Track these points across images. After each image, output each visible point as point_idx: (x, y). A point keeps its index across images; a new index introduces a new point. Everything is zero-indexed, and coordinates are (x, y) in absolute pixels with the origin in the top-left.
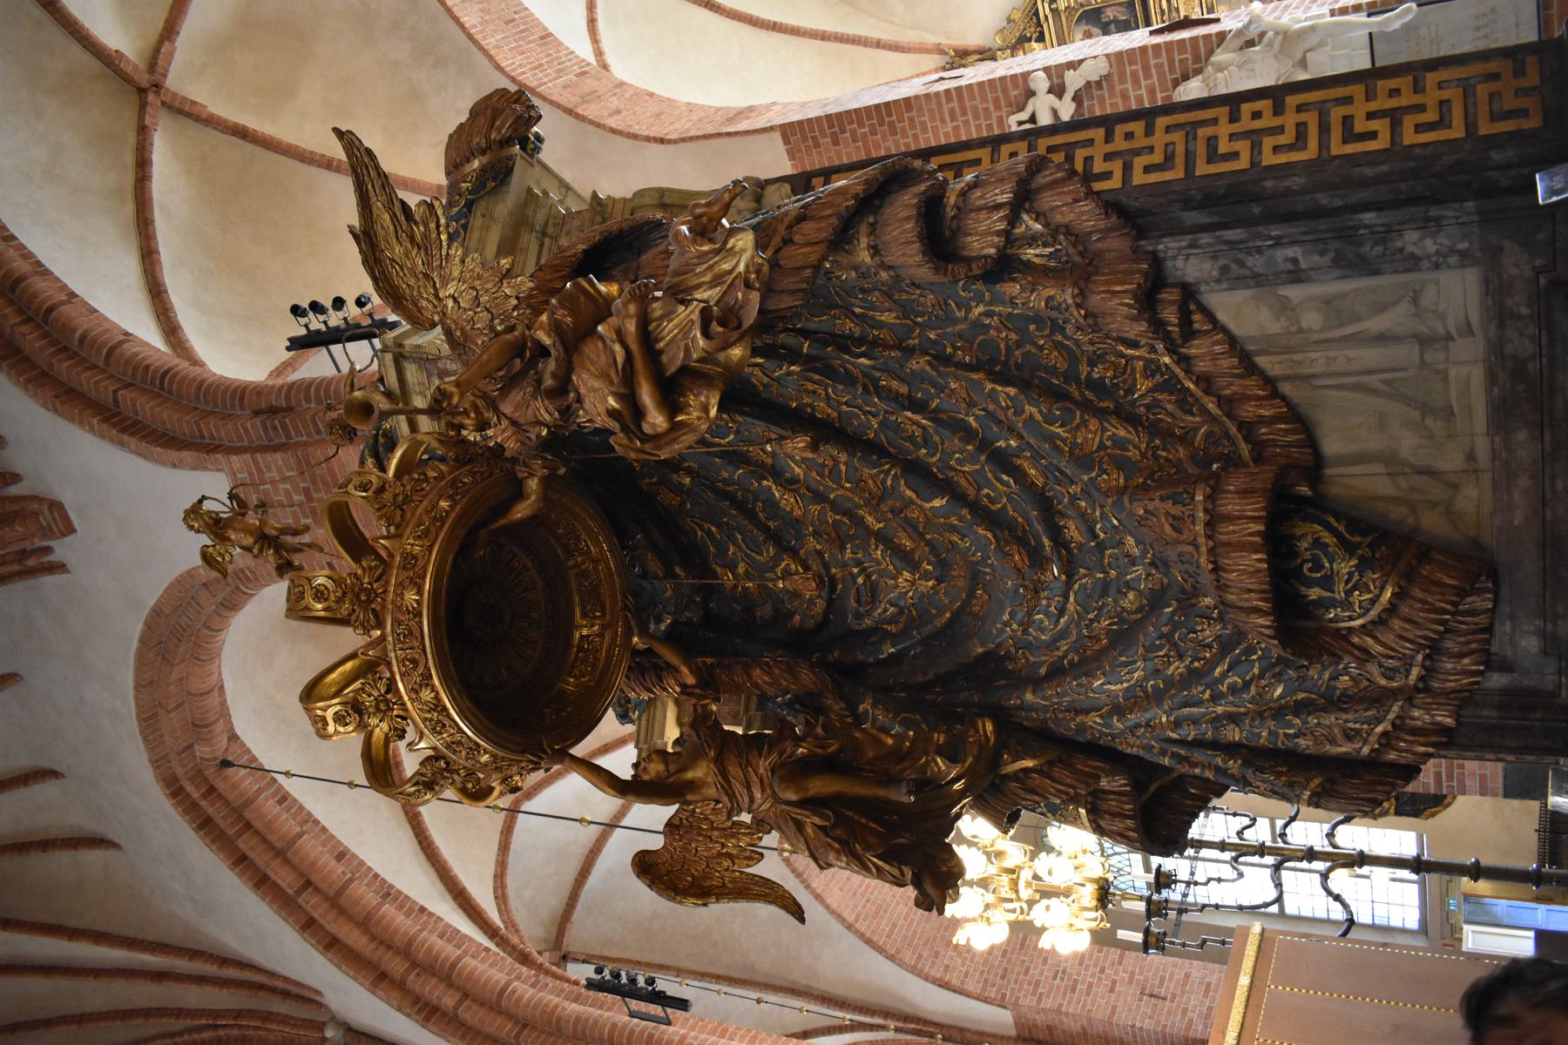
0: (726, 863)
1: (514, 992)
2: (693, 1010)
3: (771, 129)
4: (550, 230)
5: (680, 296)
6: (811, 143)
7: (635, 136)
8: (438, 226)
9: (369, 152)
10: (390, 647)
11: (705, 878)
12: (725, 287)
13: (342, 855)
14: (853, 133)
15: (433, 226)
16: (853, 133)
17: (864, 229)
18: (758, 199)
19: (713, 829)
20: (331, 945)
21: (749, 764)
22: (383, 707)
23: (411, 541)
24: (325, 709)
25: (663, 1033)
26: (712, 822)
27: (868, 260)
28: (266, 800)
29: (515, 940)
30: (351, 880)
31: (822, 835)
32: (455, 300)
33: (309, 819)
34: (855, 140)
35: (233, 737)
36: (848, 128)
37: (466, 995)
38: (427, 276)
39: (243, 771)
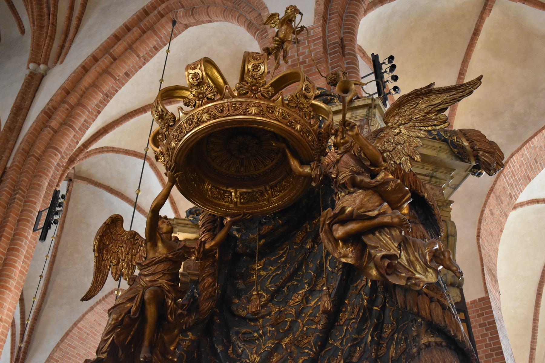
0: (114, 262)
1: (56, 155)
2: (39, 243)
3: (487, 292)
4: (434, 180)
5: (402, 244)
6: (480, 312)
7: (480, 222)
8: (435, 125)
9: (471, 92)
10: (229, 100)
11: (107, 251)
12: (407, 267)
13: (128, 75)
14: (486, 335)
15: (435, 123)
16: (486, 335)
17: (439, 340)
18: (452, 285)
19: (132, 256)
20: (85, 69)
21: (164, 274)
22: (201, 96)
23: (281, 111)
24: (200, 69)
25: (29, 228)
26: (135, 255)
27: (423, 342)
28: (156, 41)
29: (81, 156)
30: (115, 79)
31: (126, 311)
32: (399, 133)
33: (146, 60)
34: (482, 336)
35: (186, 27)
36: (489, 332)
37: (56, 132)
38: (410, 120)
39: (170, 30)
